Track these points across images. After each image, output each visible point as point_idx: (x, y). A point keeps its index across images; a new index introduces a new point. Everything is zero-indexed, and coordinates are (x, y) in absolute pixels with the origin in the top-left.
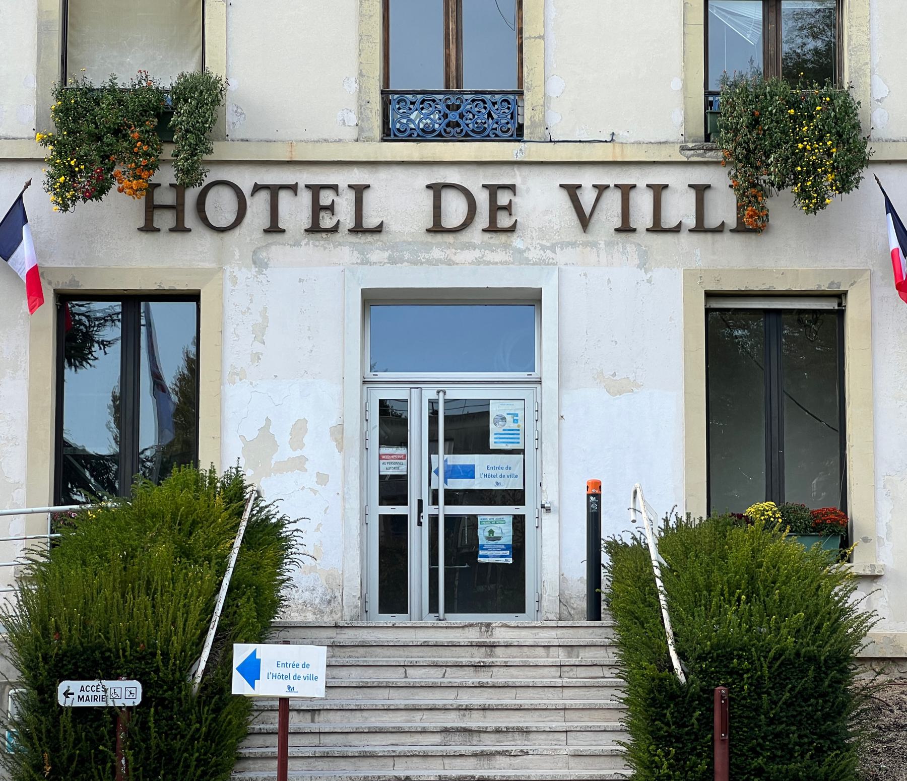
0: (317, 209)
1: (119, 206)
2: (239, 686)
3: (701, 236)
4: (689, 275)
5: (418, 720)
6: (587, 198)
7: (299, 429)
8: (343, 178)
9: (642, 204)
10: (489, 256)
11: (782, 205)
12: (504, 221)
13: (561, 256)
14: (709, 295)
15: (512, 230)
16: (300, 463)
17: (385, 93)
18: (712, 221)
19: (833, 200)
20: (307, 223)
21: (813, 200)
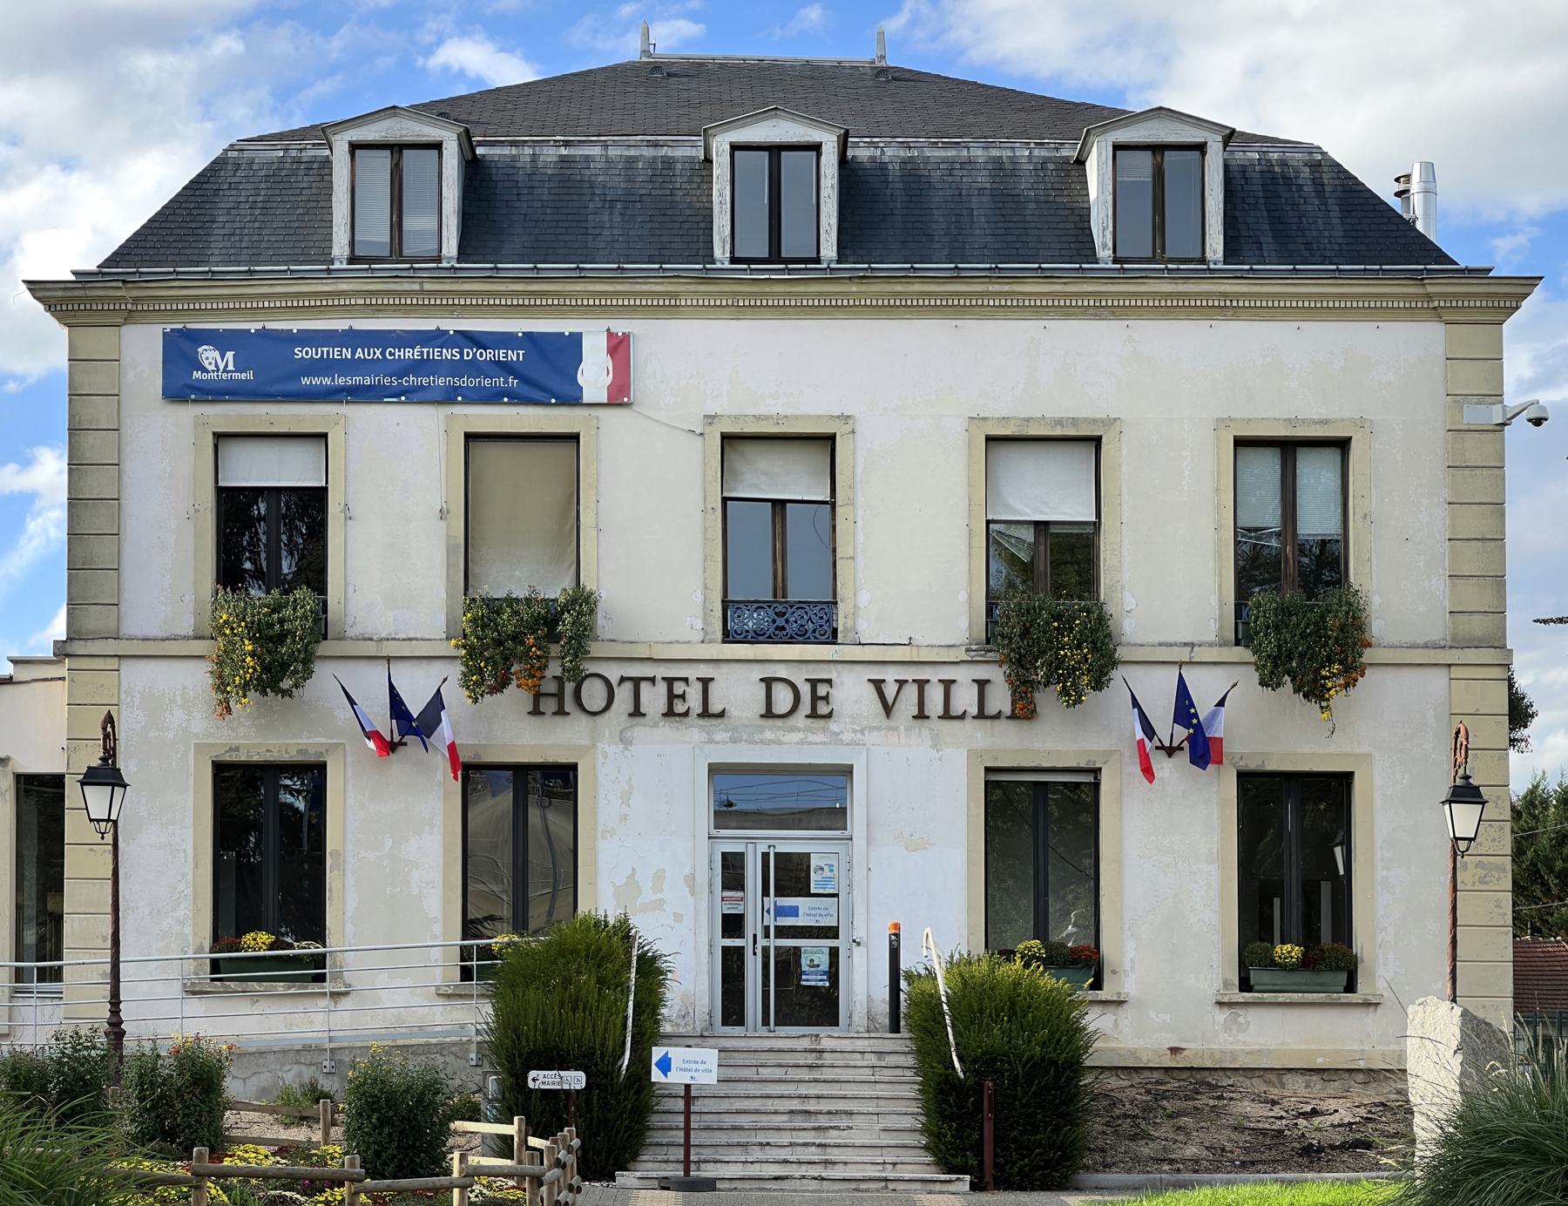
0: (672, 697)
1: (515, 697)
2: (656, 1075)
3: (982, 722)
4: (971, 754)
5: (771, 1105)
6: (890, 690)
7: (659, 877)
8: (692, 672)
9: (935, 696)
10: (811, 738)
11: (1047, 699)
12: (823, 709)
13: (869, 738)
14: (988, 770)
15: (829, 716)
16: (659, 905)
17: (726, 604)
18: (991, 709)
19: (1090, 697)
20: (663, 708)
21: (1072, 696)
